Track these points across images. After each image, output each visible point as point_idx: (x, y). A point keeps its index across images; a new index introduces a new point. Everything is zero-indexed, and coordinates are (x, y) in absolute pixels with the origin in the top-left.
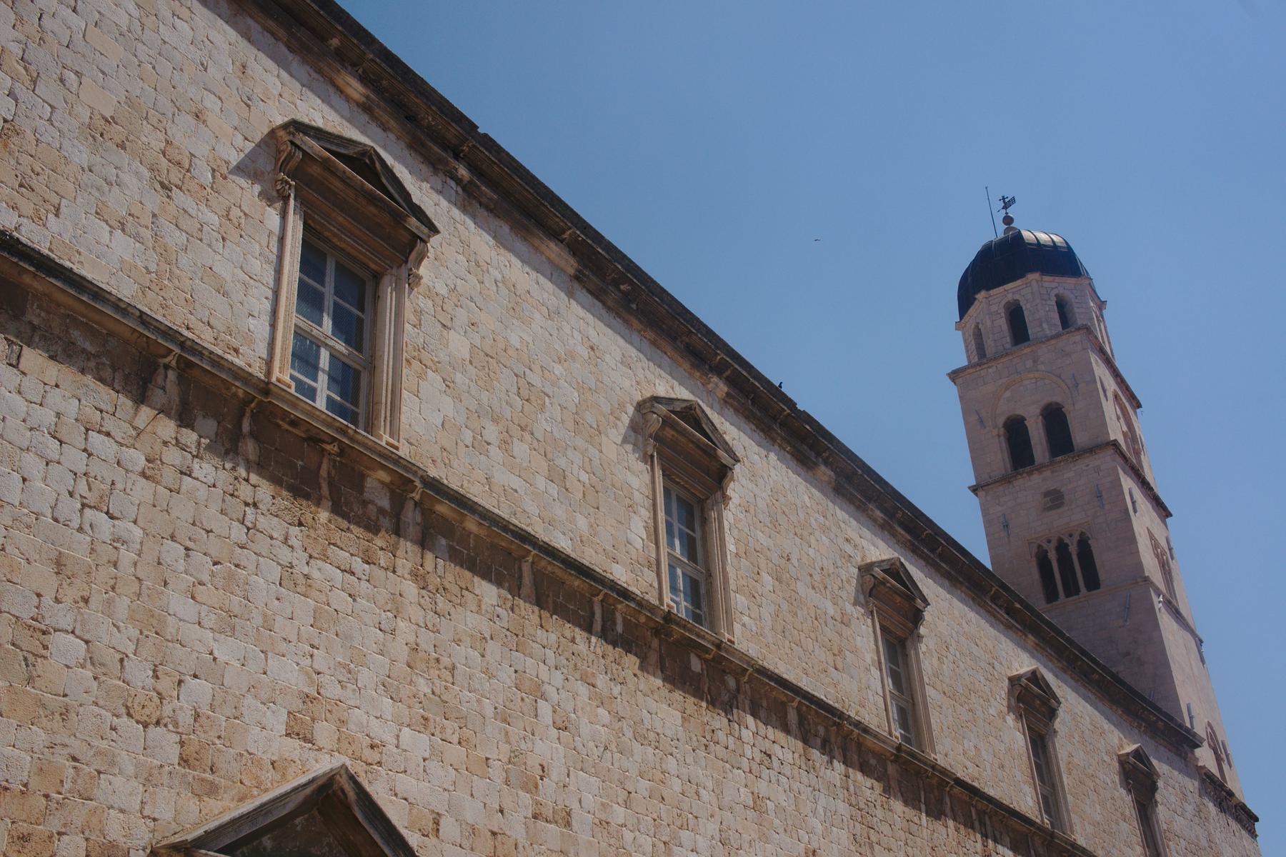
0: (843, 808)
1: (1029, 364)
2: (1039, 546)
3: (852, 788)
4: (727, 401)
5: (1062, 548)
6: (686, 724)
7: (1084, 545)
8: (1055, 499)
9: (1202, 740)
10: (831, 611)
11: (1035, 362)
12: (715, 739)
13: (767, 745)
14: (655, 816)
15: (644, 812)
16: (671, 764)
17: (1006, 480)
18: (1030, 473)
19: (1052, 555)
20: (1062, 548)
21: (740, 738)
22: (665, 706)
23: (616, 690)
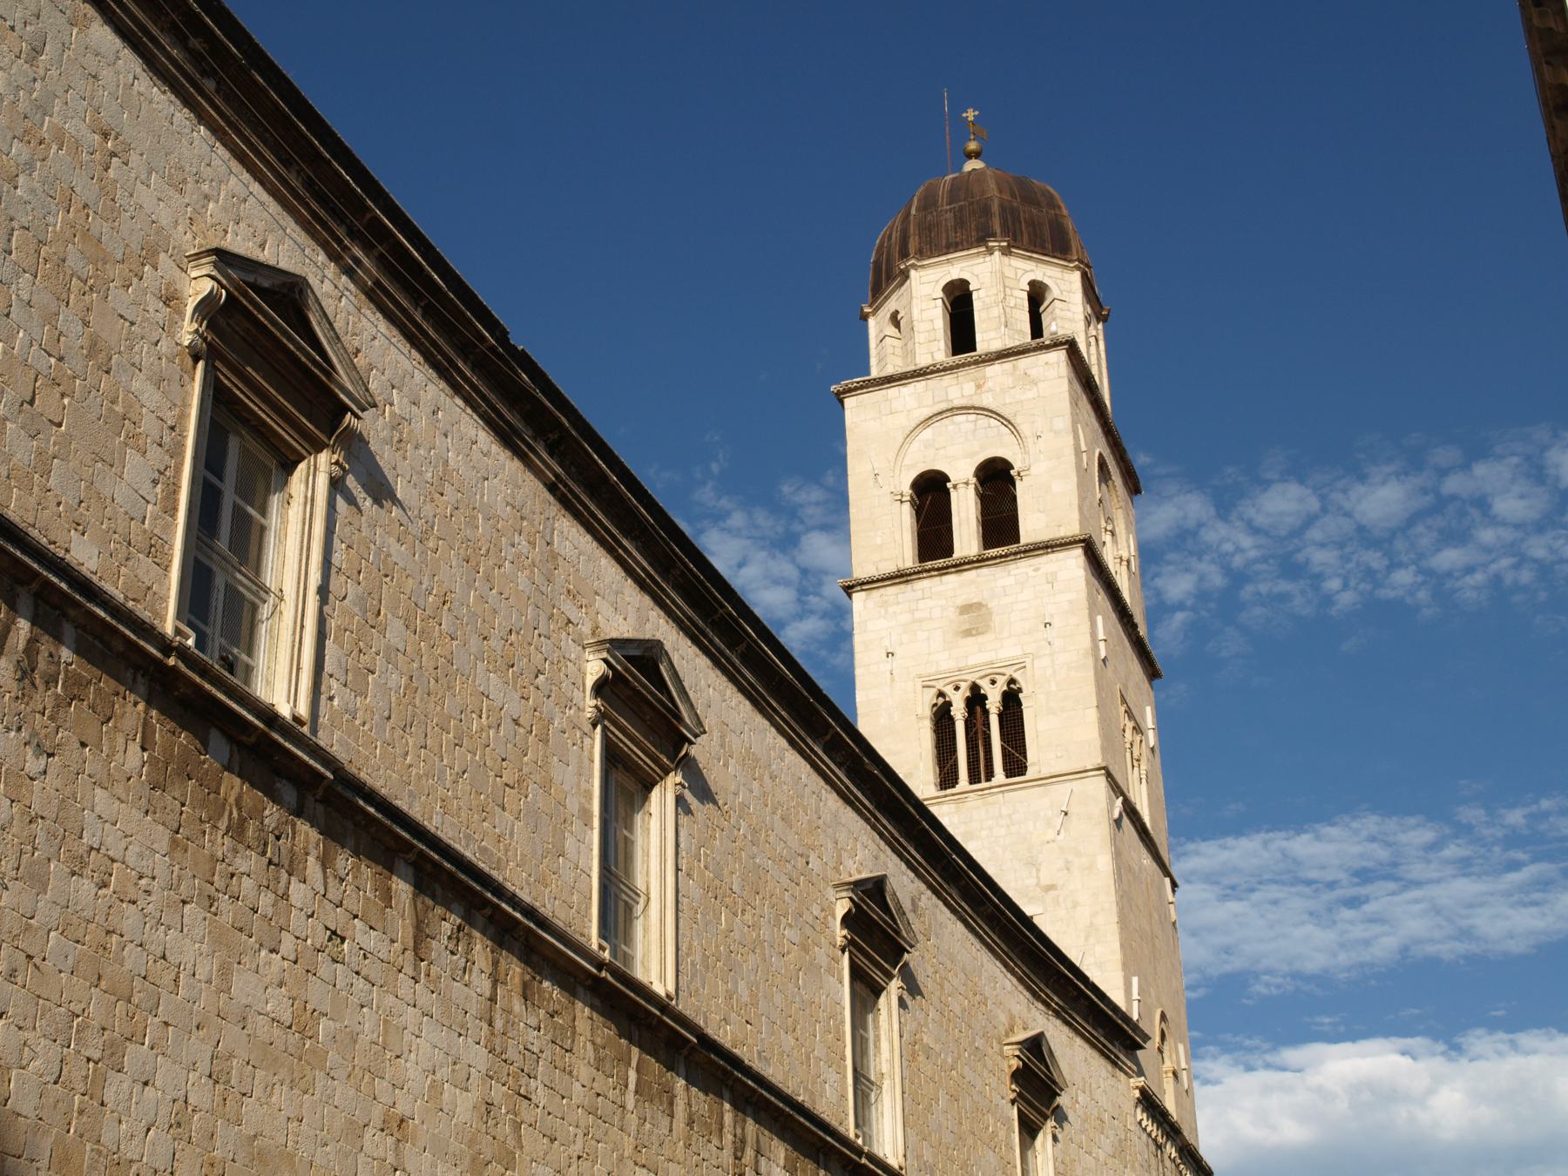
0: (478, 1057)
1: (969, 388)
3: (499, 1024)
4: (375, 296)
5: (976, 699)
6: (178, 854)
7: (1012, 699)
8: (975, 618)
9: (1146, 1038)
10: (513, 707)
11: (979, 387)
12: (234, 888)
13: (336, 918)
14: (77, 1008)
15: (55, 997)
16: (129, 920)
17: (900, 577)
18: (943, 571)
19: (959, 712)
20: (976, 699)
21: (285, 896)
22: (137, 814)
23: (34, 764)
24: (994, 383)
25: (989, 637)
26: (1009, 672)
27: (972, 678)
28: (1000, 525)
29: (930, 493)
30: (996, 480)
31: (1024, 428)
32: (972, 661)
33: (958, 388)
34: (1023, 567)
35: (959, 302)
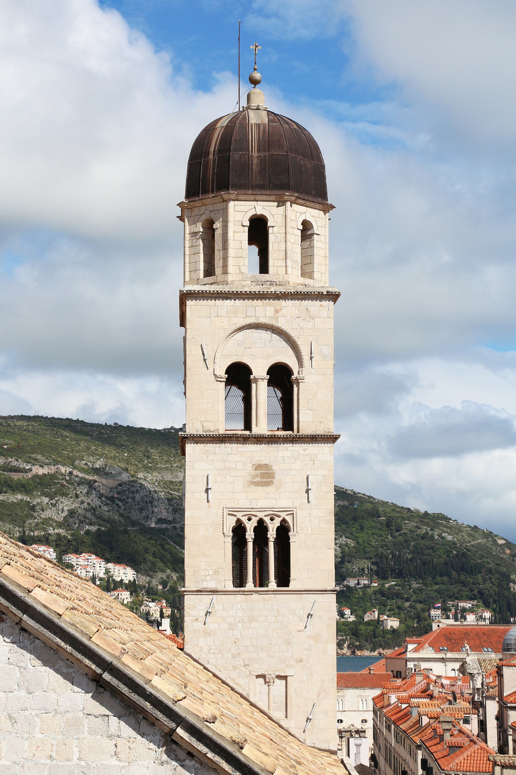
2: (239, 521)
7: (283, 531)
8: (265, 476)
18: (244, 440)
19: (250, 535)
25: (271, 489)
26: (283, 515)
27: (261, 515)
30: (281, 377)
32: (261, 504)
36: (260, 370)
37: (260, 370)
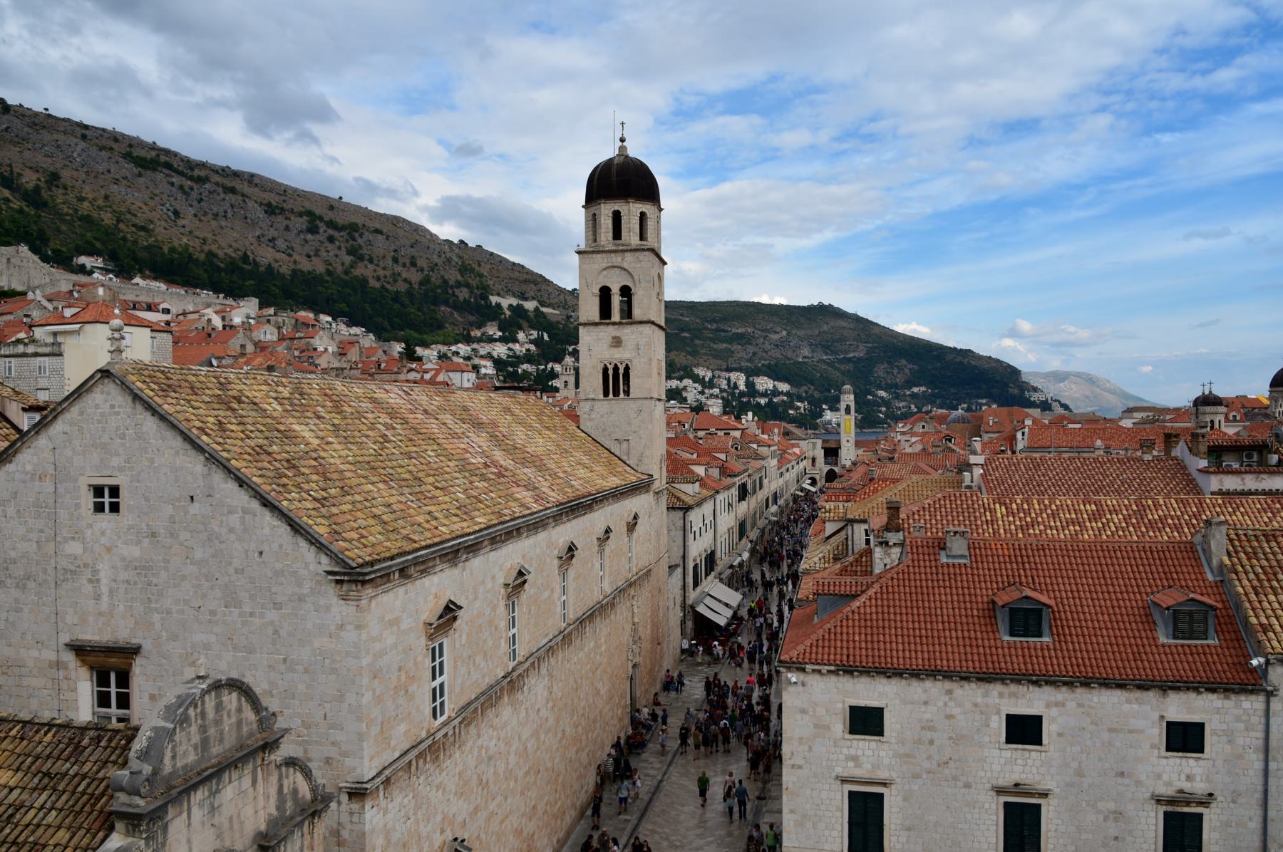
1: (619, 259)
5: (616, 368)
7: (627, 369)
8: (617, 342)
17: (596, 324)
19: (611, 372)
20: (616, 368)
24: (628, 260)
28: (627, 312)
29: (605, 293)
31: (636, 278)
32: (617, 356)
33: (616, 259)
34: (634, 328)
35: (617, 217)
36: (615, 290)
37: (615, 290)
